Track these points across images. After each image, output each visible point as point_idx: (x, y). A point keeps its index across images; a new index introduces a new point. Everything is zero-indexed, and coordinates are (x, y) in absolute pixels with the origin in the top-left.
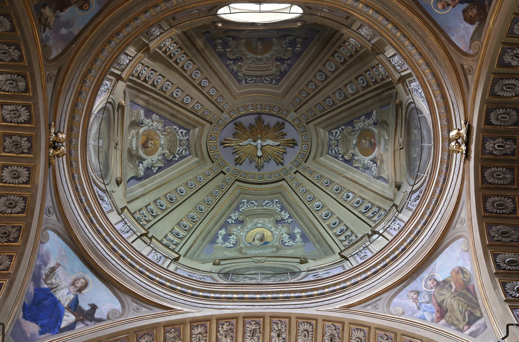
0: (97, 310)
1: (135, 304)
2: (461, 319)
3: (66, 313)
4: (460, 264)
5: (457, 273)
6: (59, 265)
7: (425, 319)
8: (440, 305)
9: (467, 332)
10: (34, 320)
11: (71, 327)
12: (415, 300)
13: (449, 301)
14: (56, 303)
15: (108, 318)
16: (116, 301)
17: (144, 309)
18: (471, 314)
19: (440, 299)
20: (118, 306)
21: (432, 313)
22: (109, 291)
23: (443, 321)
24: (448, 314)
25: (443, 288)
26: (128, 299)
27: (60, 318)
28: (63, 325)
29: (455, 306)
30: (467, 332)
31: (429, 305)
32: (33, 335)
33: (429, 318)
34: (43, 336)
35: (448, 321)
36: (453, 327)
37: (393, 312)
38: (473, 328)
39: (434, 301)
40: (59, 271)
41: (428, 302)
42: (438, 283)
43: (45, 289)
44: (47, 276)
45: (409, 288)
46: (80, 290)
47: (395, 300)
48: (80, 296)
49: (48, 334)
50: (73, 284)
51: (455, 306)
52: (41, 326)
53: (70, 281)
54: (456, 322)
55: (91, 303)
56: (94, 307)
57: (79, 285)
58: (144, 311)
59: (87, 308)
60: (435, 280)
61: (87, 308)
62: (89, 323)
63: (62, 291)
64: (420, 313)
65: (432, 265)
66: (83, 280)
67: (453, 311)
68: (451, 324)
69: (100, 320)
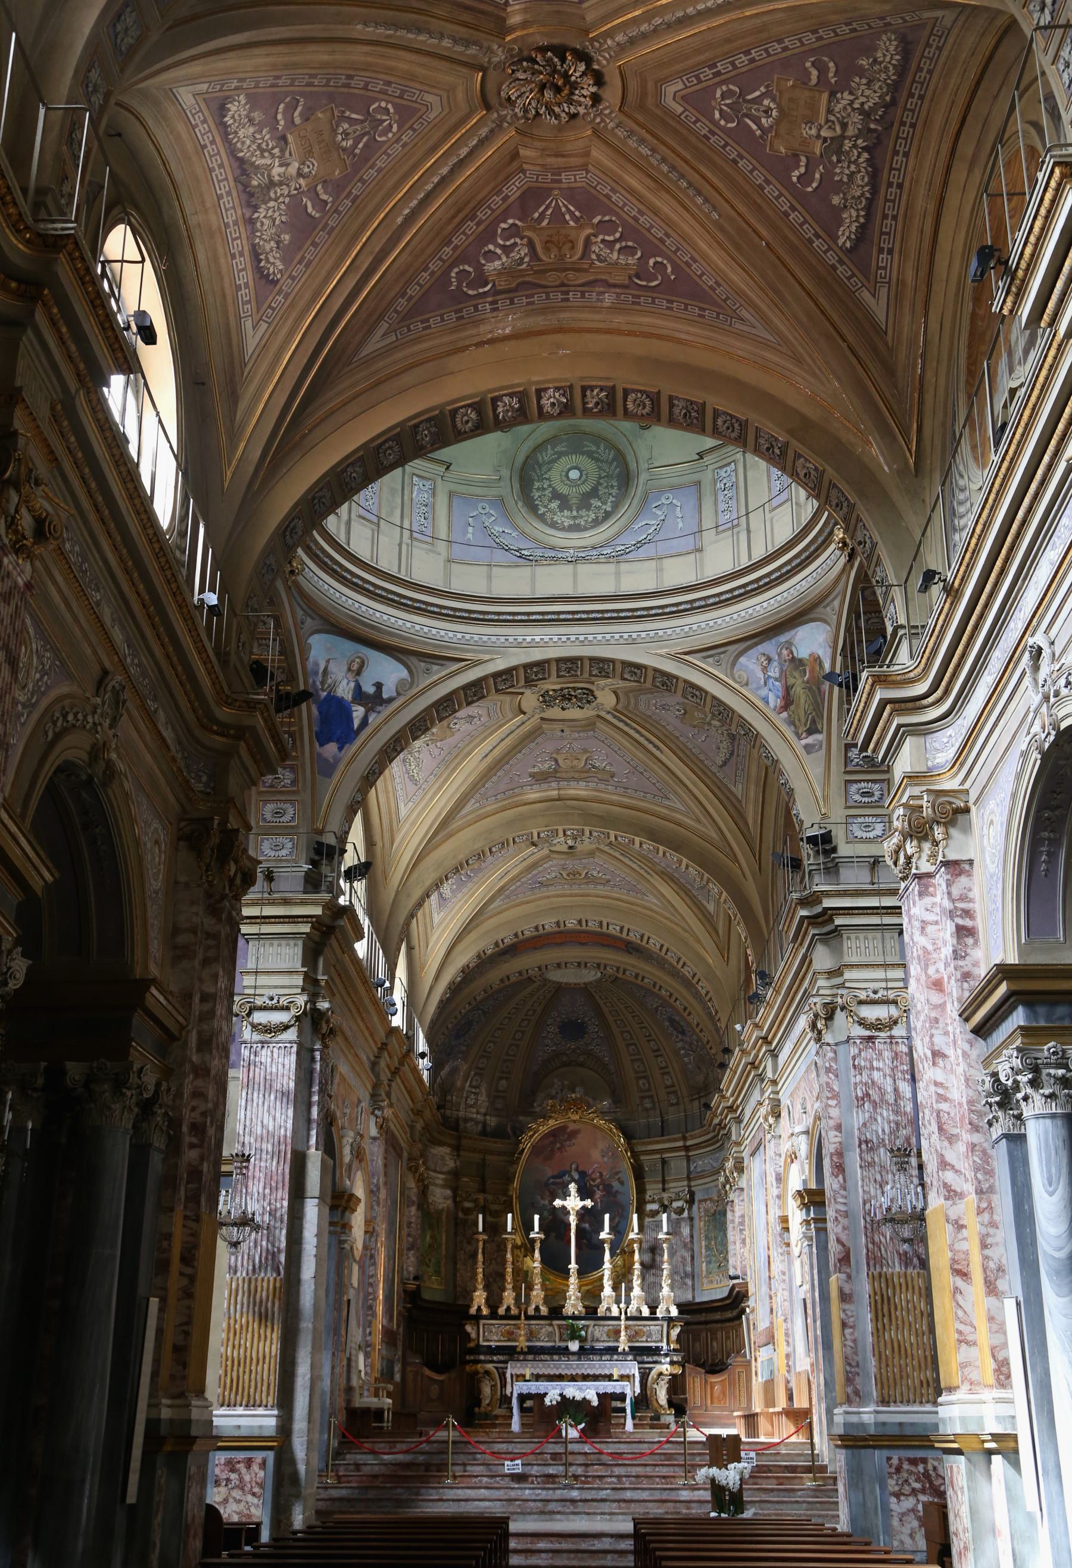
0: (384, 689)
1: (423, 664)
2: (803, 720)
3: (354, 709)
4: (820, 653)
5: (815, 660)
6: (328, 661)
7: (767, 703)
8: (788, 689)
9: (803, 742)
10: (329, 740)
11: (364, 723)
12: (765, 669)
13: (798, 689)
14: (340, 701)
15: (399, 694)
16: (402, 667)
17: (435, 668)
18: (813, 722)
19: (791, 681)
20: (404, 673)
21: (778, 697)
22: (389, 658)
23: (785, 715)
24: (792, 708)
25: (796, 668)
26: (413, 661)
27: (350, 719)
28: (356, 723)
29: (802, 701)
30: (803, 742)
31: (777, 683)
32: (334, 757)
33: (772, 704)
34: (343, 752)
35: (790, 716)
36: (792, 728)
37: (736, 676)
38: (810, 740)
39: (783, 681)
40: (332, 667)
41: (776, 680)
42: (793, 657)
43: (326, 697)
44: (323, 683)
45: (760, 648)
46: (359, 672)
47: (743, 660)
48: (360, 679)
49: (347, 745)
50: (349, 670)
51: (802, 701)
52: (338, 741)
53: (345, 668)
54: (797, 722)
55: (374, 682)
56: (379, 686)
57: (355, 667)
58: (438, 672)
59: (370, 690)
60: (792, 653)
61: (370, 690)
62: (379, 708)
63: (341, 686)
64: (764, 692)
65: (793, 632)
66: (358, 660)
67: (798, 706)
68: (791, 722)
69: (390, 700)
